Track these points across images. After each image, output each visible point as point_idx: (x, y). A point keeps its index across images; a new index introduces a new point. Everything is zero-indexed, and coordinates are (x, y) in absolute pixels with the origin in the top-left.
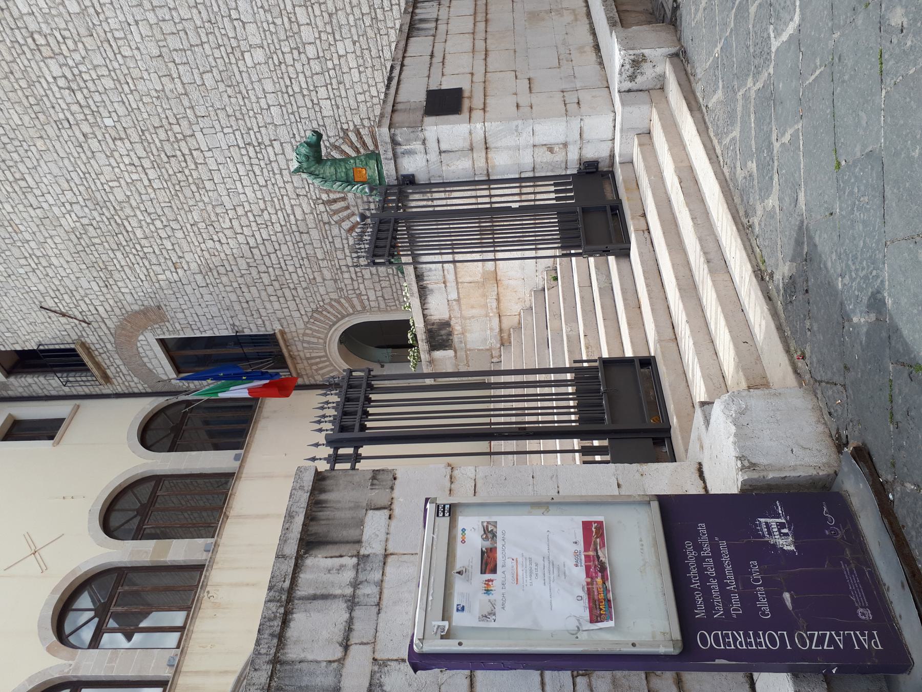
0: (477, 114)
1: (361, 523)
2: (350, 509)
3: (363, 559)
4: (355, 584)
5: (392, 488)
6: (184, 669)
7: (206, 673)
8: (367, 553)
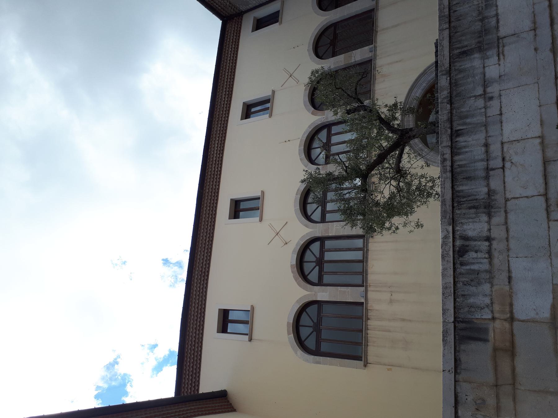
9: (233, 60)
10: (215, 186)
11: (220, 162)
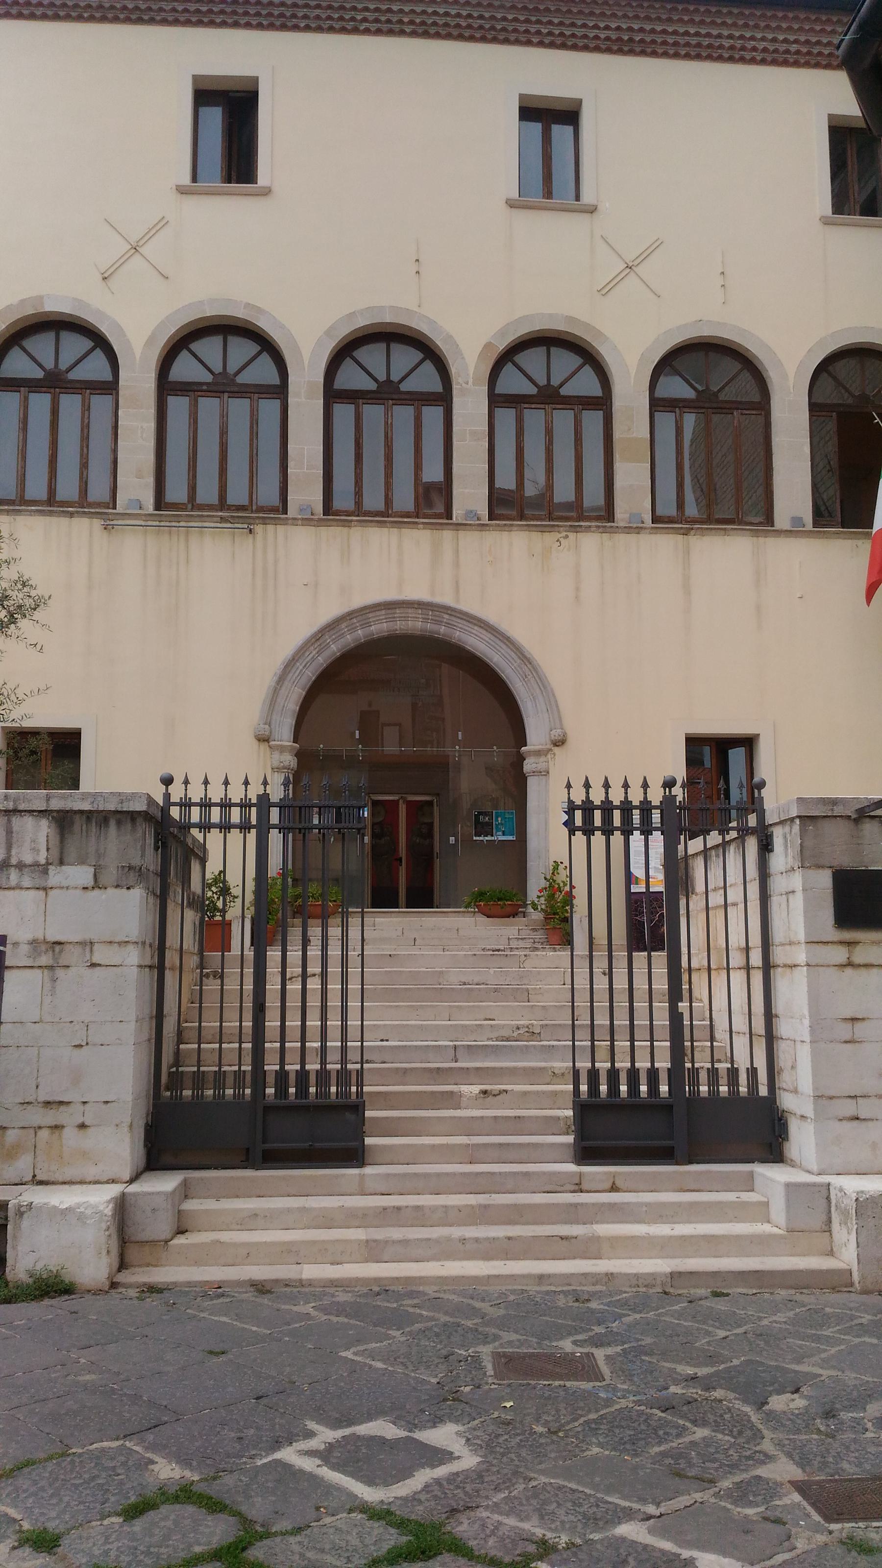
0: (840, 954)
1: (82, 861)
2: (97, 851)
3: (43, 869)
4: (21, 866)
5: (117, 886)
6: (461, 534)
7: (457, 564)
8: (50, 871)
9: (743, 48)
10: (305, 17)
11: (385, 27)
